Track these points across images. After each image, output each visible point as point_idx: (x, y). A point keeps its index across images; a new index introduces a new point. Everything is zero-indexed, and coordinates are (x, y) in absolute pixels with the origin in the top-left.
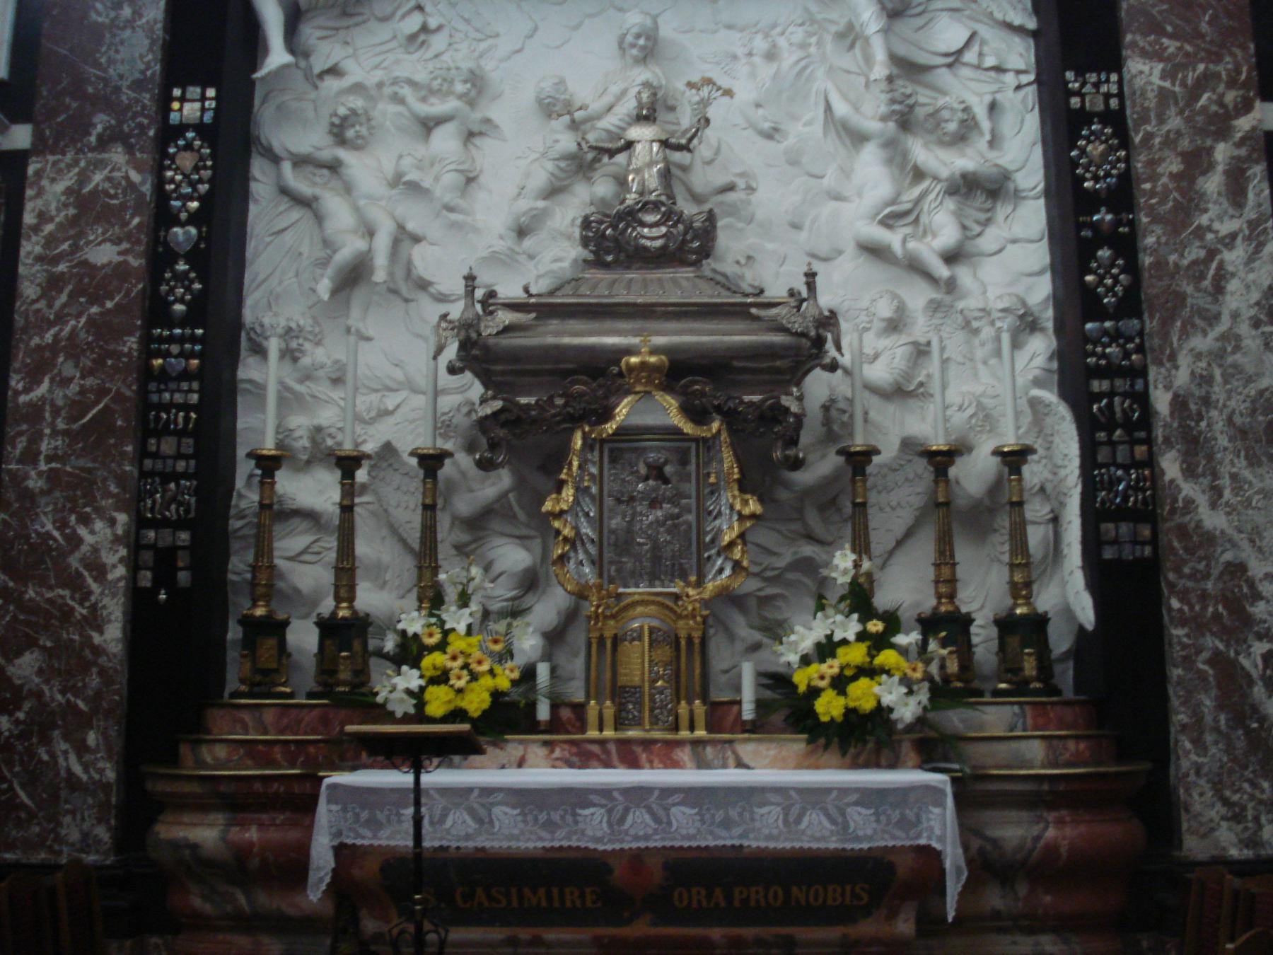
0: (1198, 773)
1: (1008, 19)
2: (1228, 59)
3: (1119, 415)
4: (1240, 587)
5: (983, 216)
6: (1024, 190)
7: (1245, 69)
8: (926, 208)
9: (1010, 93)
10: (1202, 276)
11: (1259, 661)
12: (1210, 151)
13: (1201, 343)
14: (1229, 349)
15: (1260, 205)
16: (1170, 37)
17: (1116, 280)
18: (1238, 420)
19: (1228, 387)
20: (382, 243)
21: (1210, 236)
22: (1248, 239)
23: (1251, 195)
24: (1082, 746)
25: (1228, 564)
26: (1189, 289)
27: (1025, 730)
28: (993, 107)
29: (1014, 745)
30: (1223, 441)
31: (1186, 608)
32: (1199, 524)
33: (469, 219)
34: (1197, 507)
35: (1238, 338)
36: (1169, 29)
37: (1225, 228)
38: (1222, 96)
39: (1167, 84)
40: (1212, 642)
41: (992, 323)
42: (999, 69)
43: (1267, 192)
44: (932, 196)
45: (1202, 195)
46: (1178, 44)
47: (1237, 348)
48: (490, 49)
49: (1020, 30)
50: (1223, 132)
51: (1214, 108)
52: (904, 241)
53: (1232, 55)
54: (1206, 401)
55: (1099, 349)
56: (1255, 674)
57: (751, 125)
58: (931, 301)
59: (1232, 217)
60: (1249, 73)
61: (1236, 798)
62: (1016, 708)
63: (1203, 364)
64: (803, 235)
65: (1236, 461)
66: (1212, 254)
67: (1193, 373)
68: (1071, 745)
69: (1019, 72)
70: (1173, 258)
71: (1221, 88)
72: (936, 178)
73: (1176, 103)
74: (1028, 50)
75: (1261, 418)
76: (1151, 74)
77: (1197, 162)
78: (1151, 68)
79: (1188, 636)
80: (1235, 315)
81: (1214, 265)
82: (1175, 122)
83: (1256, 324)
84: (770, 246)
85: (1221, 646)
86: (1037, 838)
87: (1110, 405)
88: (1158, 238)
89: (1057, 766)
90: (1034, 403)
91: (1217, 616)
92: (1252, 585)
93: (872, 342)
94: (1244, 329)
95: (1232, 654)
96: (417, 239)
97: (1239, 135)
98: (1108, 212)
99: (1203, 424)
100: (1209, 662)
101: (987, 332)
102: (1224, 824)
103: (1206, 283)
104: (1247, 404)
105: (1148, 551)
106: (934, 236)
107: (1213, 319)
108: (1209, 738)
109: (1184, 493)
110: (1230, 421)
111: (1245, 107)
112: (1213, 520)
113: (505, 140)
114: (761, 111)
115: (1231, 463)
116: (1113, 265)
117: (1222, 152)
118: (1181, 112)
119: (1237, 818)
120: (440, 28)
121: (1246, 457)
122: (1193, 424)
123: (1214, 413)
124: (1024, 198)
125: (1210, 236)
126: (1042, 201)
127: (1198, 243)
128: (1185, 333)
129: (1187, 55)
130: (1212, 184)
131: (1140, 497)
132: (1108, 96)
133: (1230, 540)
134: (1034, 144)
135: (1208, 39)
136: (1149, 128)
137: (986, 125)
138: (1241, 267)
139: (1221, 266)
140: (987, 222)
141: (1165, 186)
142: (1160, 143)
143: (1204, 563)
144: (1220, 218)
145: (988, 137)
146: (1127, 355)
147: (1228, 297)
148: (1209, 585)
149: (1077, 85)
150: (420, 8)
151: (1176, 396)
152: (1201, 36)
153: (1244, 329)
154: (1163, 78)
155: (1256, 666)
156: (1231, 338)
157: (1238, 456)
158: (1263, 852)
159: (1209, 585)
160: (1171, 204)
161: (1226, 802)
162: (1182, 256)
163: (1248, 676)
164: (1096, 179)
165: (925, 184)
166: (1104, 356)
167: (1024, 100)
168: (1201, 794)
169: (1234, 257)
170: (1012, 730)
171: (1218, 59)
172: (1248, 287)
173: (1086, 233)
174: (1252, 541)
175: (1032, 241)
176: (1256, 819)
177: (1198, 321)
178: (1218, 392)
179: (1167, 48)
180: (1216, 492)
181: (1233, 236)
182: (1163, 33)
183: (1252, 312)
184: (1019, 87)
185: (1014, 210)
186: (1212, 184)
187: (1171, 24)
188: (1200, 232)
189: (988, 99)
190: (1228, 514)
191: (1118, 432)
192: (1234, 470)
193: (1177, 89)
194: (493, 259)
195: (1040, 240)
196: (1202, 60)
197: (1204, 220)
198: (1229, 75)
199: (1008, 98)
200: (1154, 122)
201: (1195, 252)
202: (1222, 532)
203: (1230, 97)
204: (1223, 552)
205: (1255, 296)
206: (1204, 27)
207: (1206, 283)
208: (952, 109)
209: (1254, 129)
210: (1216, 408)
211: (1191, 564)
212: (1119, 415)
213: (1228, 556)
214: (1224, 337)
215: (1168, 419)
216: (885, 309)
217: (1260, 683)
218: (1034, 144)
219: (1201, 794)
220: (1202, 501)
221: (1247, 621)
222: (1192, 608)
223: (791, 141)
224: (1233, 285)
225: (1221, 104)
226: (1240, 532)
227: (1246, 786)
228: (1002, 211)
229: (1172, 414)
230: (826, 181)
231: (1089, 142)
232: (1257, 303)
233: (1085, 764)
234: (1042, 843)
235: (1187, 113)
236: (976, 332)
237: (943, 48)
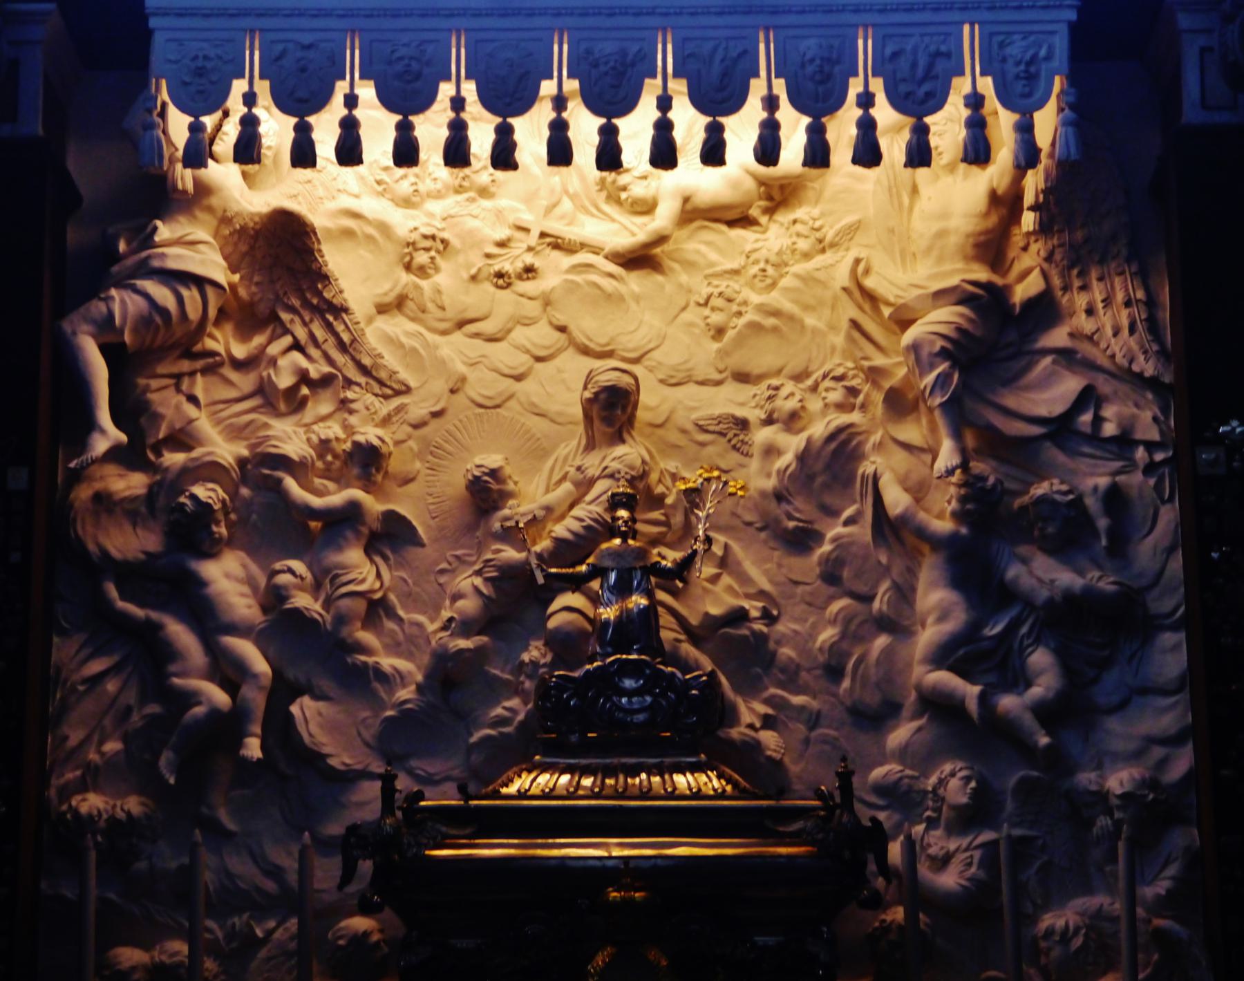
1: (1135, 368)
8: (1016, 646)
9: (1137, 478)
20: (256, 699)
28: (1114, 498)
33: (370, 660)
42: (1124, 442)
44: (1024, 630)
48: (399, 409)
49: (1152, 383)
52: (983, 698)
57: (770, 526)
58: (1023, 780)
64: (846, 683)
69: (1150, 446)
72: (1028, 603)
74: (1165, 410)
84: (798, 700)
90: (1159, 936)
93: (938, 842)
96: (297, 691)
101: (1103, 821)
106: (1029, 685)
113: (422, 545)
114: (785, 506)
120: (326, 381)
126: (1181, 636)
134: (1171, 550)
137: (1103, 523)
145: (1104, 542)
150: (297, 346)
165: (1014, 612)
167: (1158, 488)
175: (1165, 693)
184: (1150, 468)
189: (1103, 482)
194: (406, 718)
208: (1054, 503)
216: (957, 791)
223: (827, 548)
230: (876, 605)
236: (1090, 823)
237: (1043, 411)
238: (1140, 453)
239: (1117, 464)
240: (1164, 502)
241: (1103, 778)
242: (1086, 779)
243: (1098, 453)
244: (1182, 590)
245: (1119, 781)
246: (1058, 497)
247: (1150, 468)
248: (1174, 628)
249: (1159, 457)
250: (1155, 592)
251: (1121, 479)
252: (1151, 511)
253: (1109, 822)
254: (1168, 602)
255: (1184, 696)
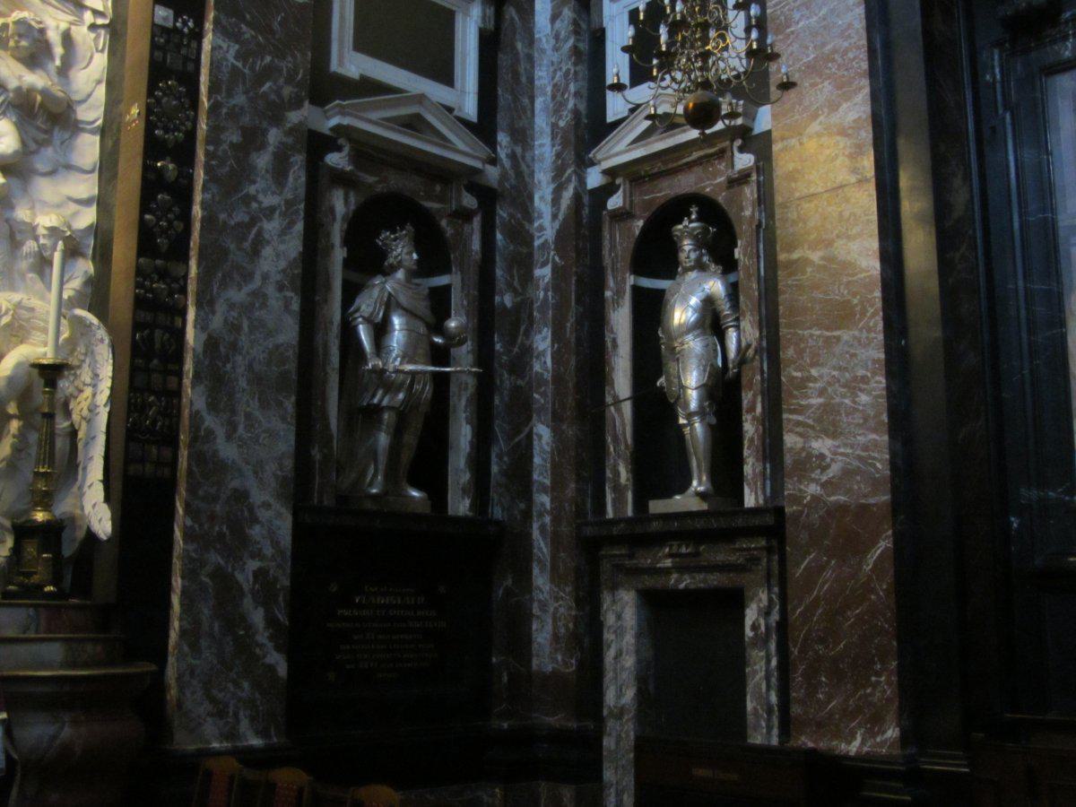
0: (192, 673)
2: (290, 59)
3: (158, 346)
4: (242, 511)
5: (42, 136)
6: (83, 122)
7: (301, 71)
9: (85, 29)
10: (244, 239)
11: (251, 579)
12: (265, 133)
13: (238, 295)
14: (257, 305)
15: (296, 189)
16: (249, 24)
17: (170, 222)
18: (257, 367)
19: (253, 337)
21: (254, 205)
22: (283, 215)
23: (291, 179)
24: (99, 648)
25: (235, 490)
26: (232, 247)
27: (37, 632)
29: (35, 648)
30: (243, 383)
31: (196, 526)
32: (215, 453)
34: (215, 438)
35: (265, 296)
36: (248, 16)
37: (269, 200)
38: (281, 88)
39: (240, 65)
40: (215, 558)
41: (36, 239)
43: (303, 179)
45: (253, 168)
46: (253, 33)
47: (264, 305)
50: (277, 120)
51: (273, 97)
53: (294, 56)
54: (234, 347)
55: (147, 283)
56: (246, 587)
59: (273, 193)
60: (304, 76)
61: (221, 696)
62: (31, 611)
63: (234, 314)
65: (251, 402)
66: (254, 220)
67: (226, 320)
68: (89, 647)
69: (96, 13)
70: (223, 216)
71: (281, 81)
73: (244, 83)
75: (274, 368)
76: (227, 52)
77: (253, 139)
78: (229, 46)
79: (195, 551)
80: (265, 277)
81: (254, 231)
82: (240, 99)
83: (281, 288)
85: (222, 562)
86: (54, 738)
87: (152, 333)
88: (213, 196)
89: (74, 666)
91: (221, 535)
92: (251, 510)
94: (271, 290)
95: (230, 570)
97: (288, 125)
98: (172, 162)
99: (229, 366)
100: (213, 576)
101: (30, 246)
102: (209, 719)
103: (247, 245)
104: (265, 355)
105: (167, 471)
107: (248, 277)
108: (204, 643)
109: (207, 423)
110: (250, 367)
111: (296, 104)
112: (228, 451)
115: (247, 403)
116: (170, 210)
117: (274, 136)
118: (246, 93)
119: (221, 714)
121: (259, 399)
122: (220, 364)
123: (239, 358)
124: (83, 130)
125: (254, 205)
127: (244, 209)
128: (224, 285)
129: (259, 44)
130: (263, 161)
131: (167, 423)
132: (186, 59)
133: (239, 470)
134: (99, 82)
135: (277, 37)
136: (219, 98)
137: (58, 50)
138: (275, 238)
139: (260, 233)
140: (46, 143)
141: (225, 152)
142: (225, 114)
143: (215, 488)
144: (265, 192)
145: (58, 62)
146: (171, 294)
147: (262, 261)
148: (218, 508)
149: (162, 40)
151: (210, 337)
152: (272, 32)
153: (271, 290)
154: (236, 58)
155: (248, 581)
156: (258, 295)
157: (254, 397)
158: (239, 744)
159: (218, 508)
160: (227, 169)
161: (213, 700)
162: (230, 216)
163: (241, 589)
164: (166, 130)
166: (152, 290)
167: (96, 40)
168: (193, 693)
169: (271, 227)
170: (24, 633)
171: (283, 57)
172: (278, 256)
173: (152, 176)
174: (256, 473)
176: (236, 715)
177: (236, 277)
178: (243, 340)
179: (244, 33)
180: (232, 427)
181: (272, 209)
182: (243, 19)
183: (279, 277)
184: (93, 27)
185: (70, 138)
186: (263, 161)
187: (249, 13)
188: (248, 199)
189: (64, 26)
190: (240, 446)
191: (155, 361)
192: (248, 409)
193: (246, 71)
195: (92, 172)
196: (270, 53)
197: (252, 190)
198: (288, 71)
199: (82, 34)
200: (223, 95)
201: (240, 216)
202: (233, 461)
203: (287, 91)
204: (232, 479)
205: (283, 264)
206: (276, 26)
207: (247, 245)
208: (30, 26)
209: (301, 123)
210: (240, 354)
211: (206, 488)
212: (158, 346)
213: (235, 484)
214: (254, 294)
215: (201, 356)
217: (250, 596)
218: (99, 82)
219: (193, 693)
220: (220, 433)
221: (244, 540)
222: (201, 525)
224: (267, 252)
225: (278, 93)
226: (248, 463)
227: (230, 685)
228: (58, 135)
229: (205, 352)
231: (165, 94)
232: (284, 271)
233: (98, 665)
234: (58, 742)
235: (251, 94)
238: (88, 17)
239: (71, 18)
240: (97, 51)
241: (34, 215)
242: (22, 213)
243: (60, 6)
244: (102, 109)
245: (46, 220)
246: (33, 23)
247: (93, 27)
248: (93, 132)
249: (100, 21)
250: (84, 106)
251: (73, 28)
252: (89, 55)
253: (36, 245)
254: (92, 112)
255: (96, 175)
